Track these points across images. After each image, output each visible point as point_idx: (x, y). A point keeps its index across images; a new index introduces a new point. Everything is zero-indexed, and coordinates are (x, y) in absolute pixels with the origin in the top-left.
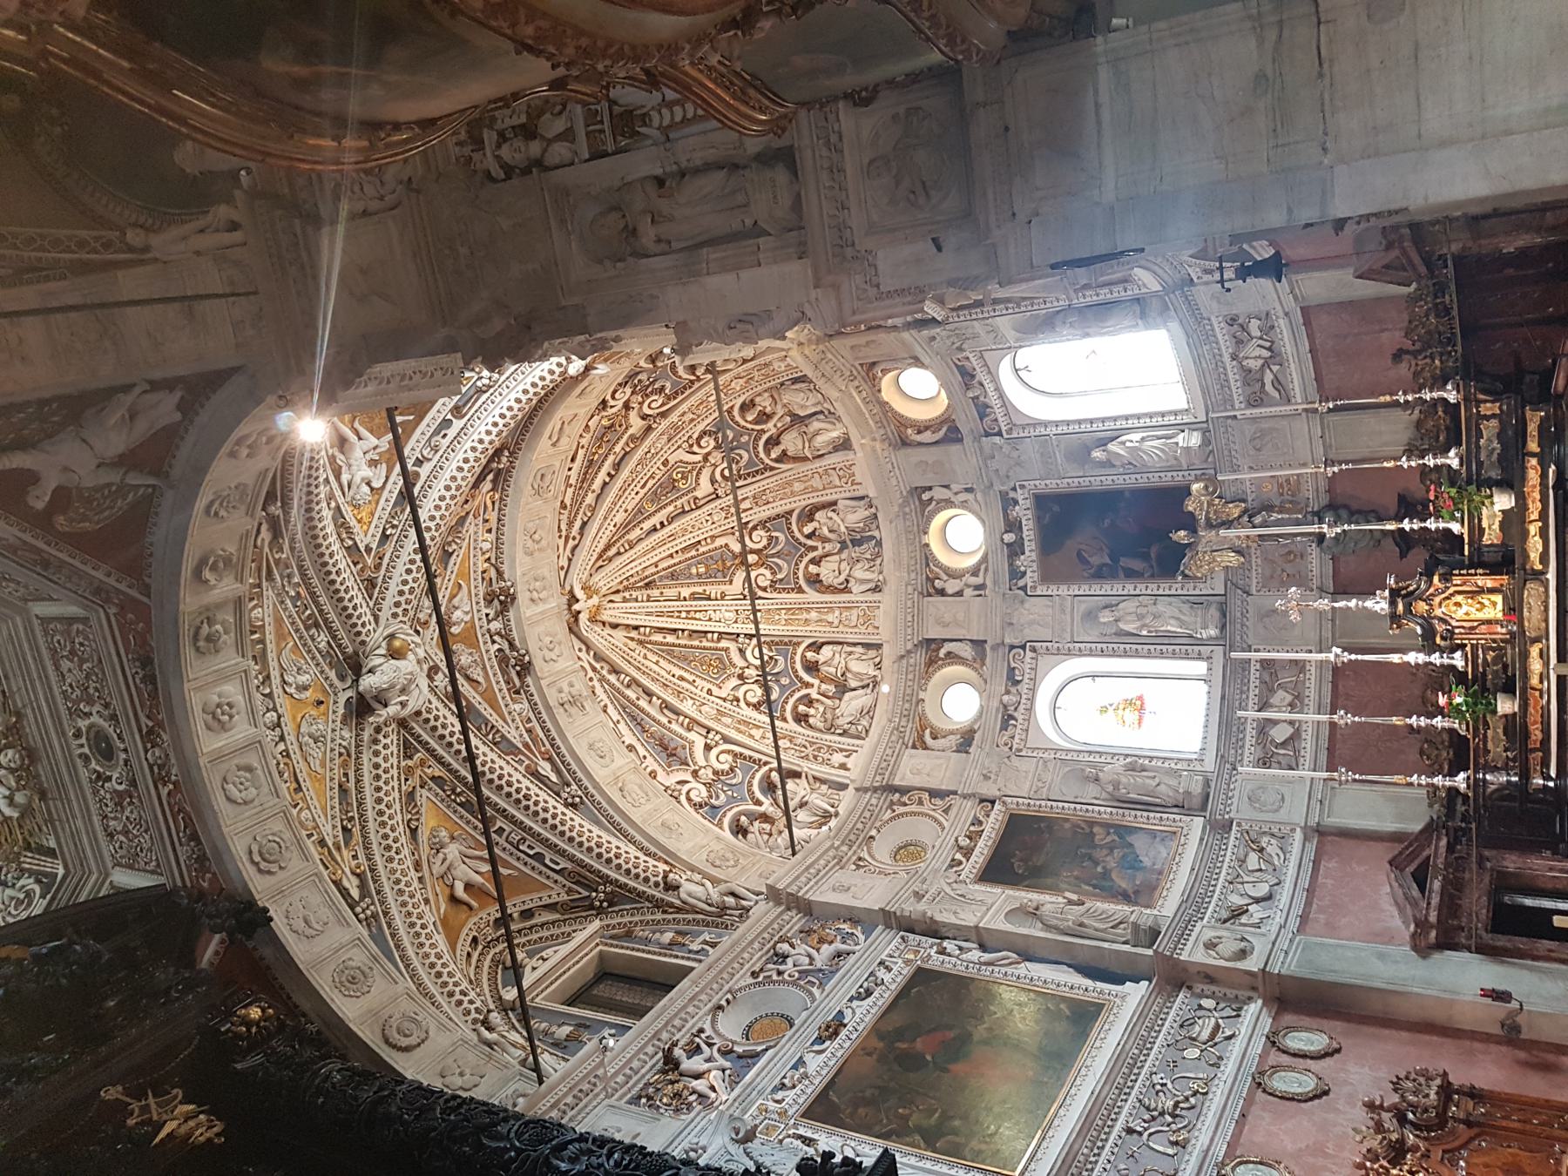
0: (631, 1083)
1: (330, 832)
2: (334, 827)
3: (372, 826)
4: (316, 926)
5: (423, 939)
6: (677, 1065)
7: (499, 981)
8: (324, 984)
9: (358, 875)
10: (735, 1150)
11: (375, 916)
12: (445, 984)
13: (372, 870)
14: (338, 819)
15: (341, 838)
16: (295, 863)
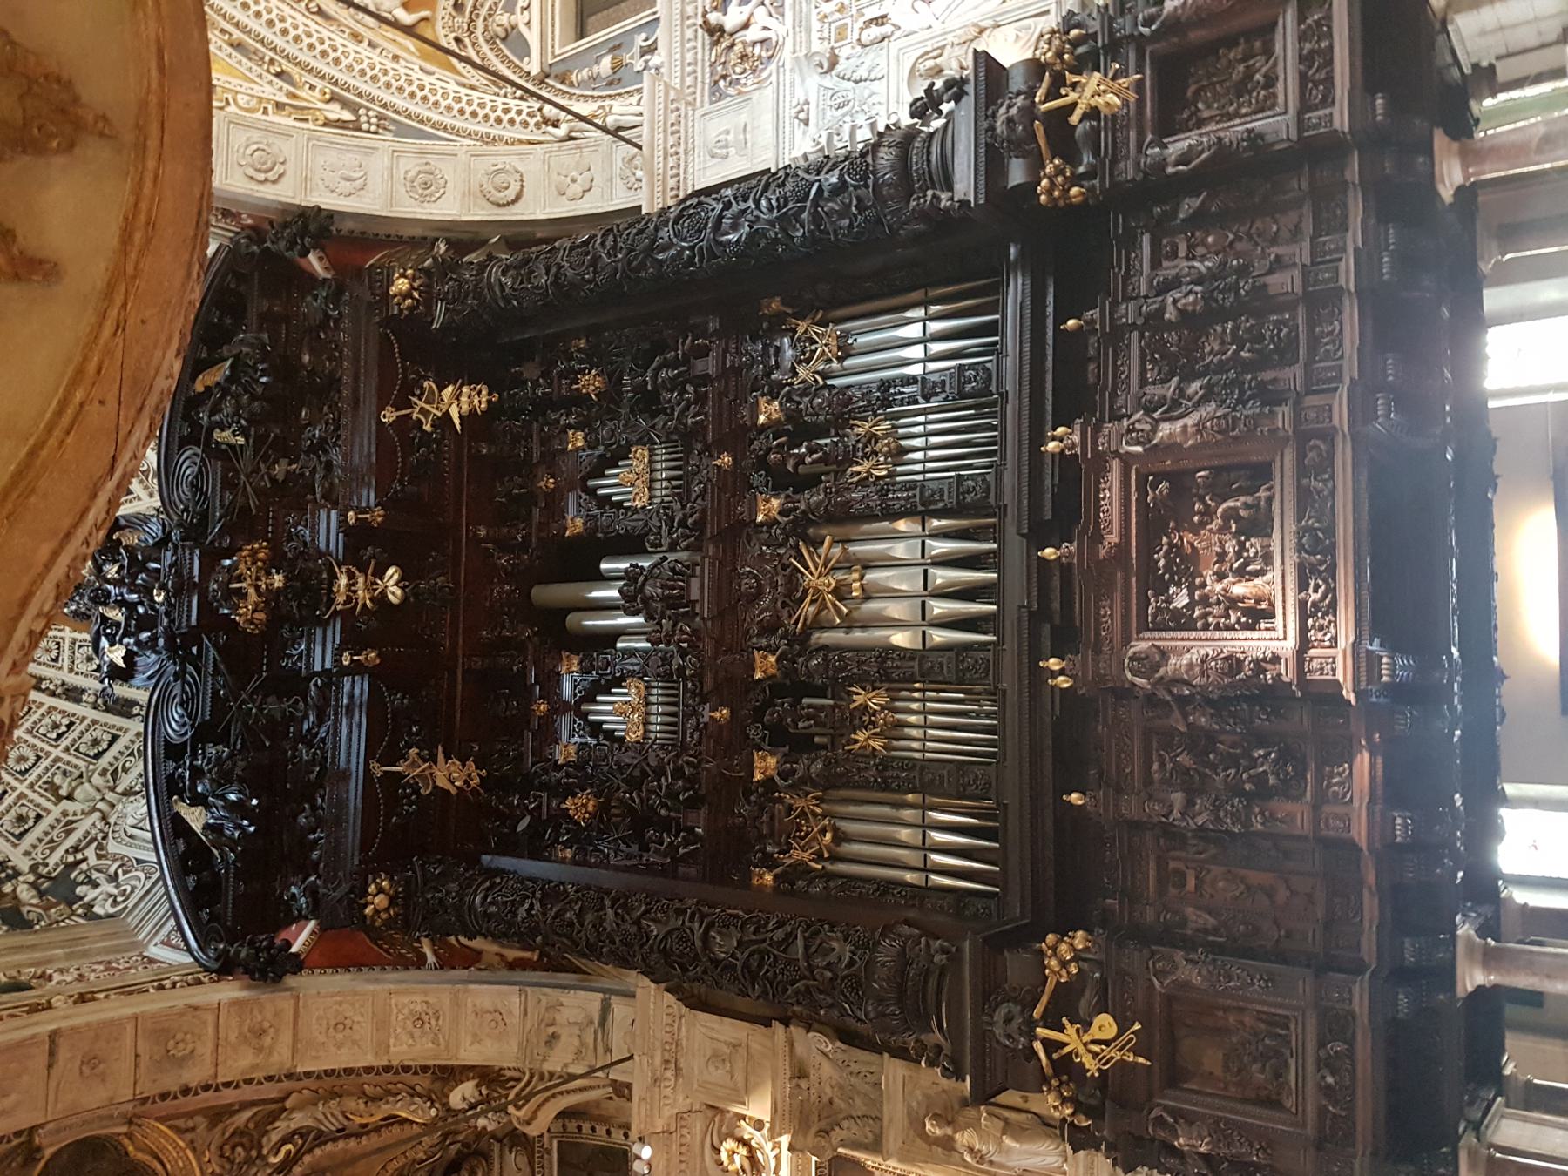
0: (699, 75)
1: (274, 91)
2: (270, 82)
3: (291, 49)
4: (356, 175)
5: (432, 99)
6: (721, 29)
7: (512, 57)
8: (410, 208)
9: (331, 100)
10: (829, 81)
11: (380, 117)
12: (486, 117)
13: (336, 83)
14: (265, 74)
15: (286, 86)
16: (285, 148)
